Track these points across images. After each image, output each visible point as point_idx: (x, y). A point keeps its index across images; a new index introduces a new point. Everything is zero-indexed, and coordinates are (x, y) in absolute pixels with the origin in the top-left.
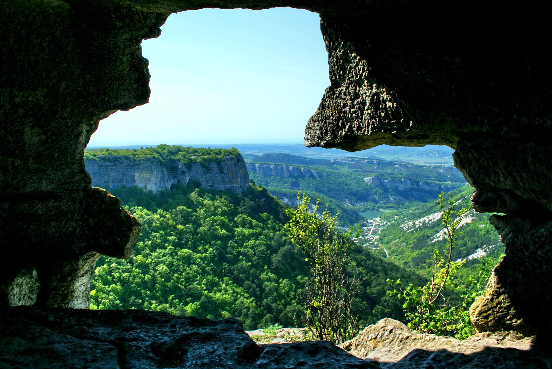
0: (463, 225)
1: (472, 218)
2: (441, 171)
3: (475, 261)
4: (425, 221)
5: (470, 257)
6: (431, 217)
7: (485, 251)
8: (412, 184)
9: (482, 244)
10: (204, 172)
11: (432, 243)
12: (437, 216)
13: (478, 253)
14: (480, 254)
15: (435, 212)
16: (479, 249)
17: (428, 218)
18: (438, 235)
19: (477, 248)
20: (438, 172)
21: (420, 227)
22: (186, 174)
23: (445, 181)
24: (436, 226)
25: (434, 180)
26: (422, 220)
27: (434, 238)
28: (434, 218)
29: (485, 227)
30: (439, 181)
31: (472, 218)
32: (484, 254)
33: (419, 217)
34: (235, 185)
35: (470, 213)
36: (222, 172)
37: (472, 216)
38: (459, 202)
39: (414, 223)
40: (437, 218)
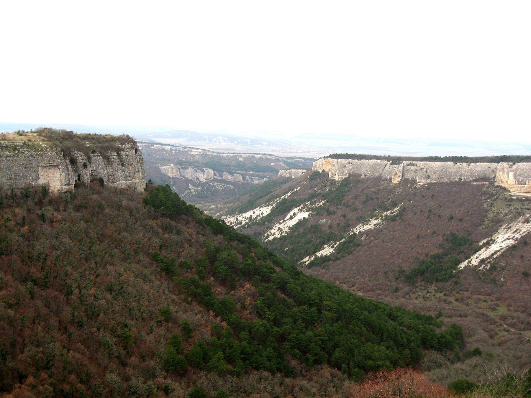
0: (300, 221)
1: (308, 213)
2: (241, 159)
3: (325, 259)
4: (251, 216)
5: (318, 254)
6: (257, 211)
7: (333, 247)
8: (215, 174)
9: (329, 240)
10: (105, 165)
11: (269, 241)
12: (265, 211)
13: (326, 249)
14: (327, 251)
15: (259, 206)
16: (325, 246)
17: (254, 213)
18: (272, 231)
19: (324, 244)
20: (238, 160)
21: (247, 223)
22: (89, 167)
23: (246, 170)
24: (268, 222)
25: (234, 169)
26: (247, 215)
27: (268, 236)
28: (262, 214)
29: (327, 221)
30: (241, 170)
31: (308, 213)
32: (332, 250)
33: (242, 211)
34: (137, 181)
35: (304, 207)
36: (123, 165)
37: (307, 211)
38: (289, 194)
39: (237, 219)
40: (265, 214)
